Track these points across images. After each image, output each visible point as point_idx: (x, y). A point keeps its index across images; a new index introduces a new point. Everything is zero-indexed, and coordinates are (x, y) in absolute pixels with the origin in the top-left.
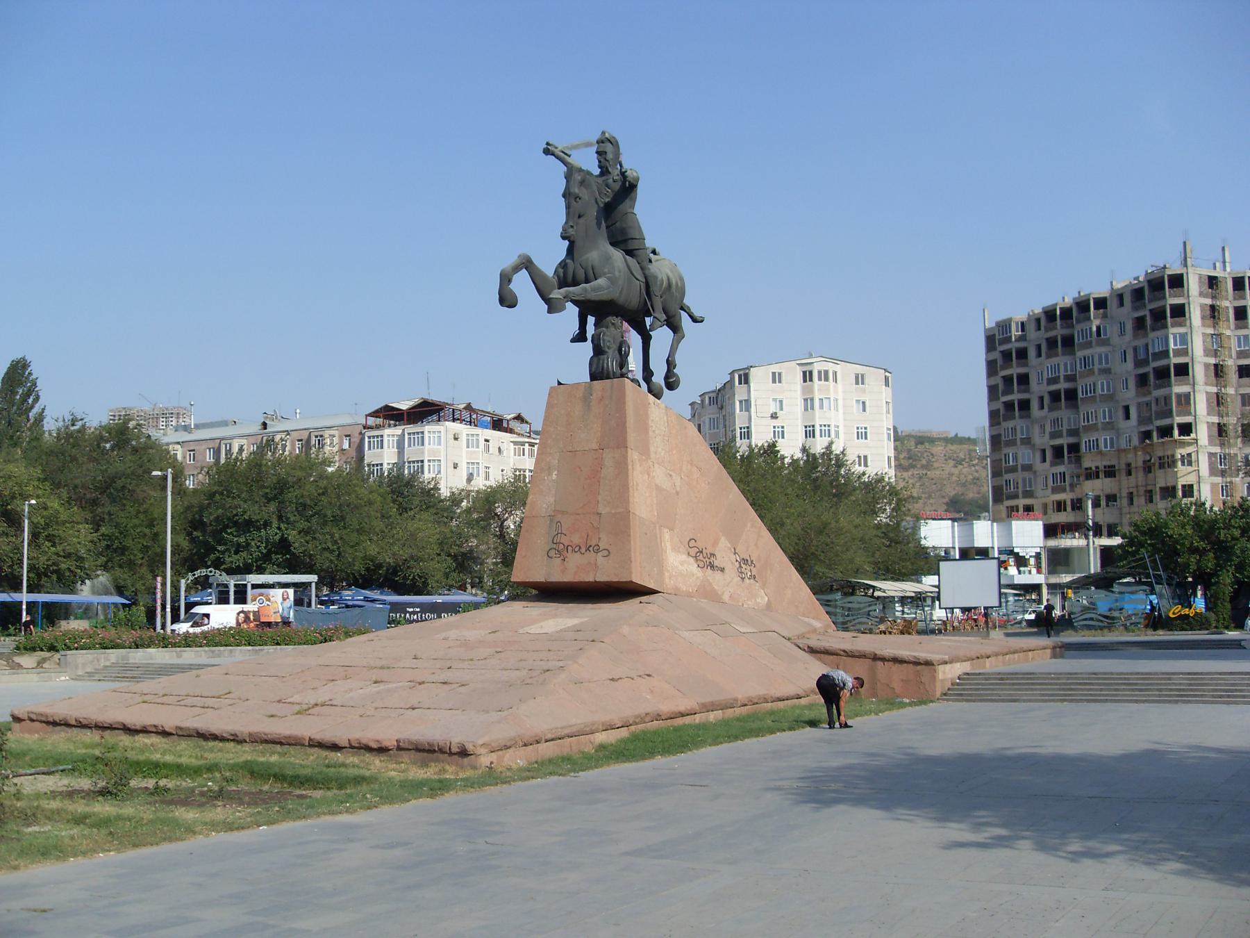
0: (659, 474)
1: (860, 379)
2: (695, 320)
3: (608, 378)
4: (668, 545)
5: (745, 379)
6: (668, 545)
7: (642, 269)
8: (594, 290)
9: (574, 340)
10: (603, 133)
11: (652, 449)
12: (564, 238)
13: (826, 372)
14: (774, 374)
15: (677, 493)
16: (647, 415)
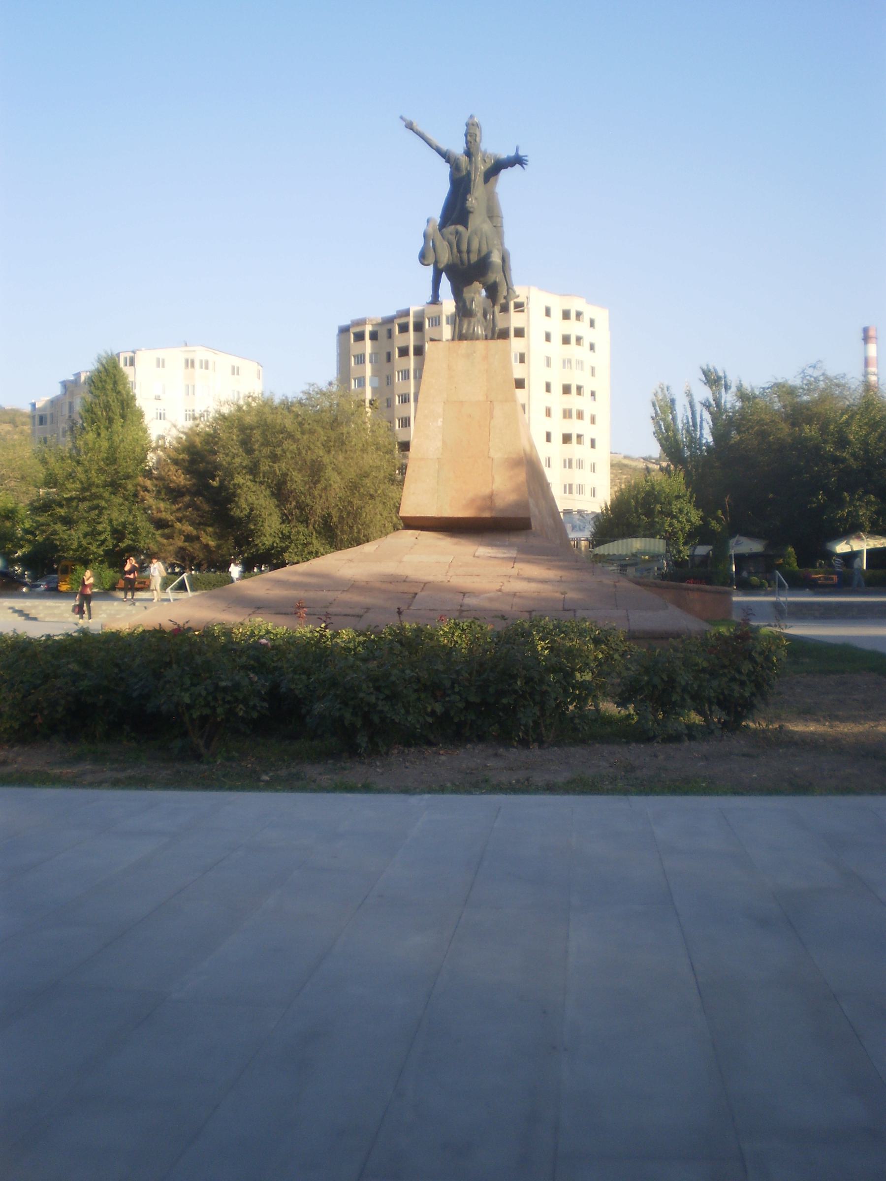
1: (235, 371)
3: (477, 339)
5: (132, 363)
10: (472, 117)
13: (207, 363)
14: (158, 360)
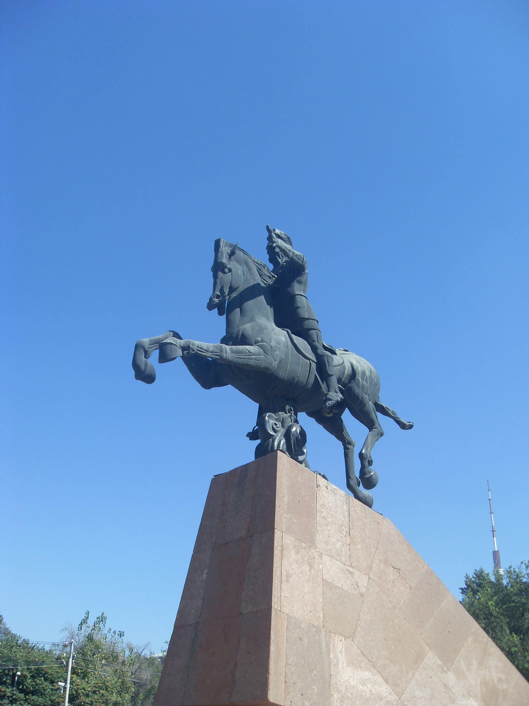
0: (331, 569)
2: (403, 426)
4: (342, 658)
6: (342, 658)
7: (314, 349)
8: (237, 352)
9: (252, 436)
11: (320, 537)
12: (211, 306)
15: (362, 595)
16: (314, 498)
